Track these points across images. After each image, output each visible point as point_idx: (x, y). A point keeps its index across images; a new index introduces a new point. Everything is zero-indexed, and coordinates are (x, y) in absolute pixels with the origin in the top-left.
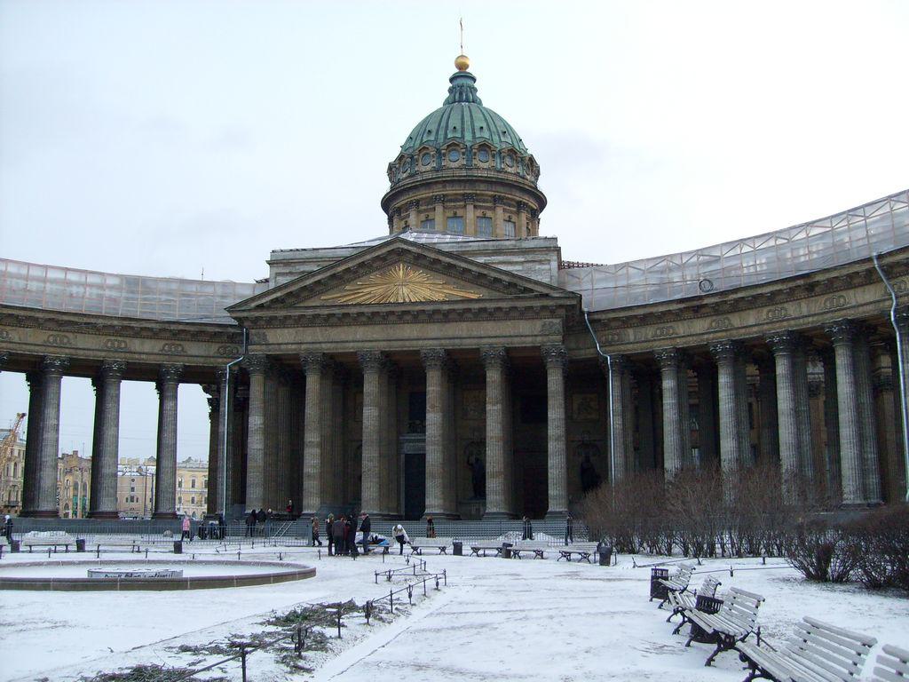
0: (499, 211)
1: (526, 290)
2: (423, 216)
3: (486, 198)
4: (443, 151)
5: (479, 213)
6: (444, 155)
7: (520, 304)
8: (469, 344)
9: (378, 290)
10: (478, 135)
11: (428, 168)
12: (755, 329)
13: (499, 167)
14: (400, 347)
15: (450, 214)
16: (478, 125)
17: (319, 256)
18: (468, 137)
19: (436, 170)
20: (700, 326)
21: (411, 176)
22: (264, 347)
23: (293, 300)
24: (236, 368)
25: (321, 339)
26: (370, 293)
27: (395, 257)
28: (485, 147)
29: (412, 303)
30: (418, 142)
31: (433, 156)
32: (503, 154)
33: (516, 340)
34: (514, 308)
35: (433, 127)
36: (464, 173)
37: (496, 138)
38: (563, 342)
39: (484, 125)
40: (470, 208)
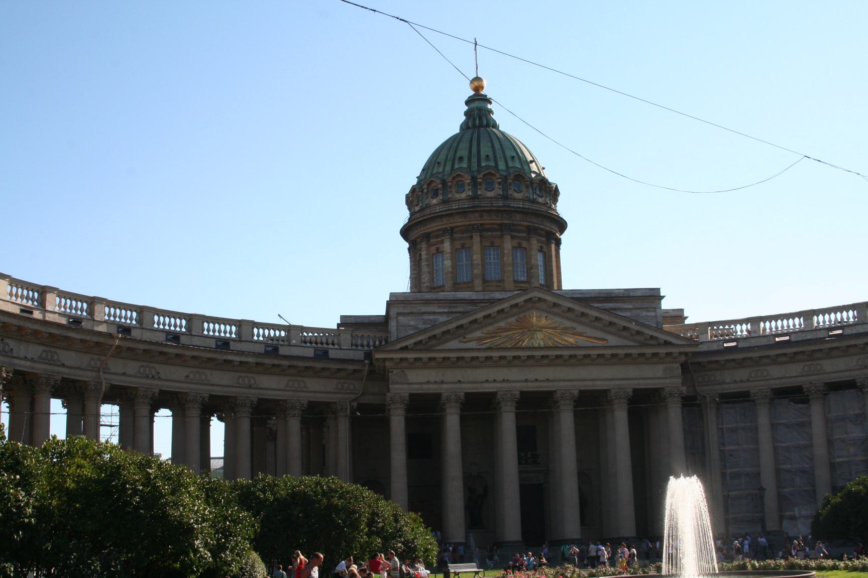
1: (652, 337)
3: (520, 228)
4: (480, 180)
5: (515, 243)
6: (480, 184)
7: (649, 351)
8: (600, 385)
10: (510, 165)
11: (463, 195)
12: (847, 373)
13: (531, 197)
14: (537, 387)
17: (440, 298)
18: (502, 166)
21: (444, 202)
22: (406, 386)
24: (355, 404)
26: (506, 336)
29: (547, 348)
30: (448, 168)
31: (468, 184)
32: (535, 185)
33: (641, 382)
35: (463, 152)
36: (501, 203)
38: (683, 384)
40: (507, 238)
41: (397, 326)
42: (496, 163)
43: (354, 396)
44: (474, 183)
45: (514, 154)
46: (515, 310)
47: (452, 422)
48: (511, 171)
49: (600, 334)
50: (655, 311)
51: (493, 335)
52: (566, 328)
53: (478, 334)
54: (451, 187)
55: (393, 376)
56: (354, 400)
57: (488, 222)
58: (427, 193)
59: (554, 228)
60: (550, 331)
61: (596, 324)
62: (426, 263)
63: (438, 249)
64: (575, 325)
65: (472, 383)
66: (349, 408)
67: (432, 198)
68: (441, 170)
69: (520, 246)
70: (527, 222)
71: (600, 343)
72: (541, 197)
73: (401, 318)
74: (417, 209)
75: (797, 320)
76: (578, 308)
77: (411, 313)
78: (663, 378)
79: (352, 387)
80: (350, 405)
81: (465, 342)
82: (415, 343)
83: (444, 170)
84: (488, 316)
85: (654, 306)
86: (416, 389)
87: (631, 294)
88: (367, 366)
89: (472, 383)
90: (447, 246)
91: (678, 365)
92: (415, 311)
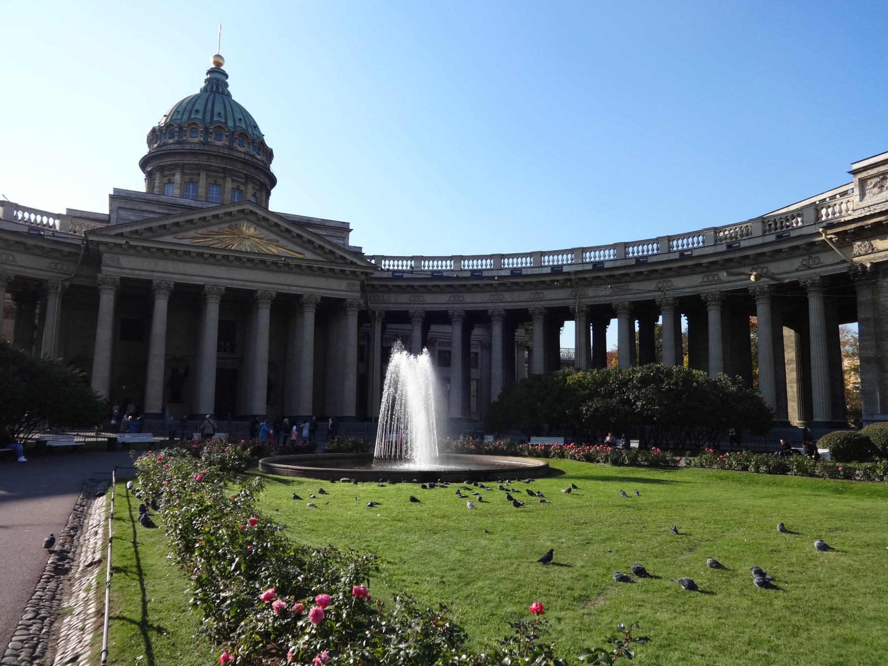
0: (250, 187)
2: (187, 178)
3: (241, 175)
5: (235, 185)
8: (294, 290)
10: (238, 124)
11: (196, 140)
12: (481, 305)
15: (211, 181)
18: (230, 123)
21: (179, 143)
22: (118, 270)
23: (150, 234)
24: (67, 284)
25: (172, 270)
26: (218, 239)
27: (242, 216)
28: (244, 135)
30: (186, 117)
31: (201, 132)
32: (255, 144)
35: (200, 106)
36: (226, 151)
37: (250, 130)
39: (242, 118)
40: (229, 180)
41: (117, 218)
43: (67, 277)
44: (206, 131)
45: (242, 118)
46: (227, 218)
47: (161, 305)
48: (238, 129)
49: (298, 249)
50: (344, 240)
51: (205, 236)
52: (270, 240)
53: (192, 233)
54: (186, 132)
55: (106, 257)
56: (66, 280)
57: (214, 164)
58: (165, 134)
59: (267, 181)
60: (257, 240)
61: (296, 240)
62: (158, 190)
63: (169, 179)
64: (278, 238)
65: (183, 274)
66: (60, 287)
67: (170, 138)
68: (179, 117)
69: (238, 189)
70: (245, 170)
71: (299, 256)
72: (259, 155)
73: (122, 212)
74: (155, 145)
75: (448, 262)
77: (132, 209)
78: (347, 291)
79: (65, 268)
80: (62, 284)
81: (179, 239)
82: (131, 232)
83: (181, 118)
85: (344, 236)
86: (127, 273)
87: (326, 224)
88: (83, 251)
89: (183, 274)
90: (177, 178)
91: (358, 282)
92: (136, 207)
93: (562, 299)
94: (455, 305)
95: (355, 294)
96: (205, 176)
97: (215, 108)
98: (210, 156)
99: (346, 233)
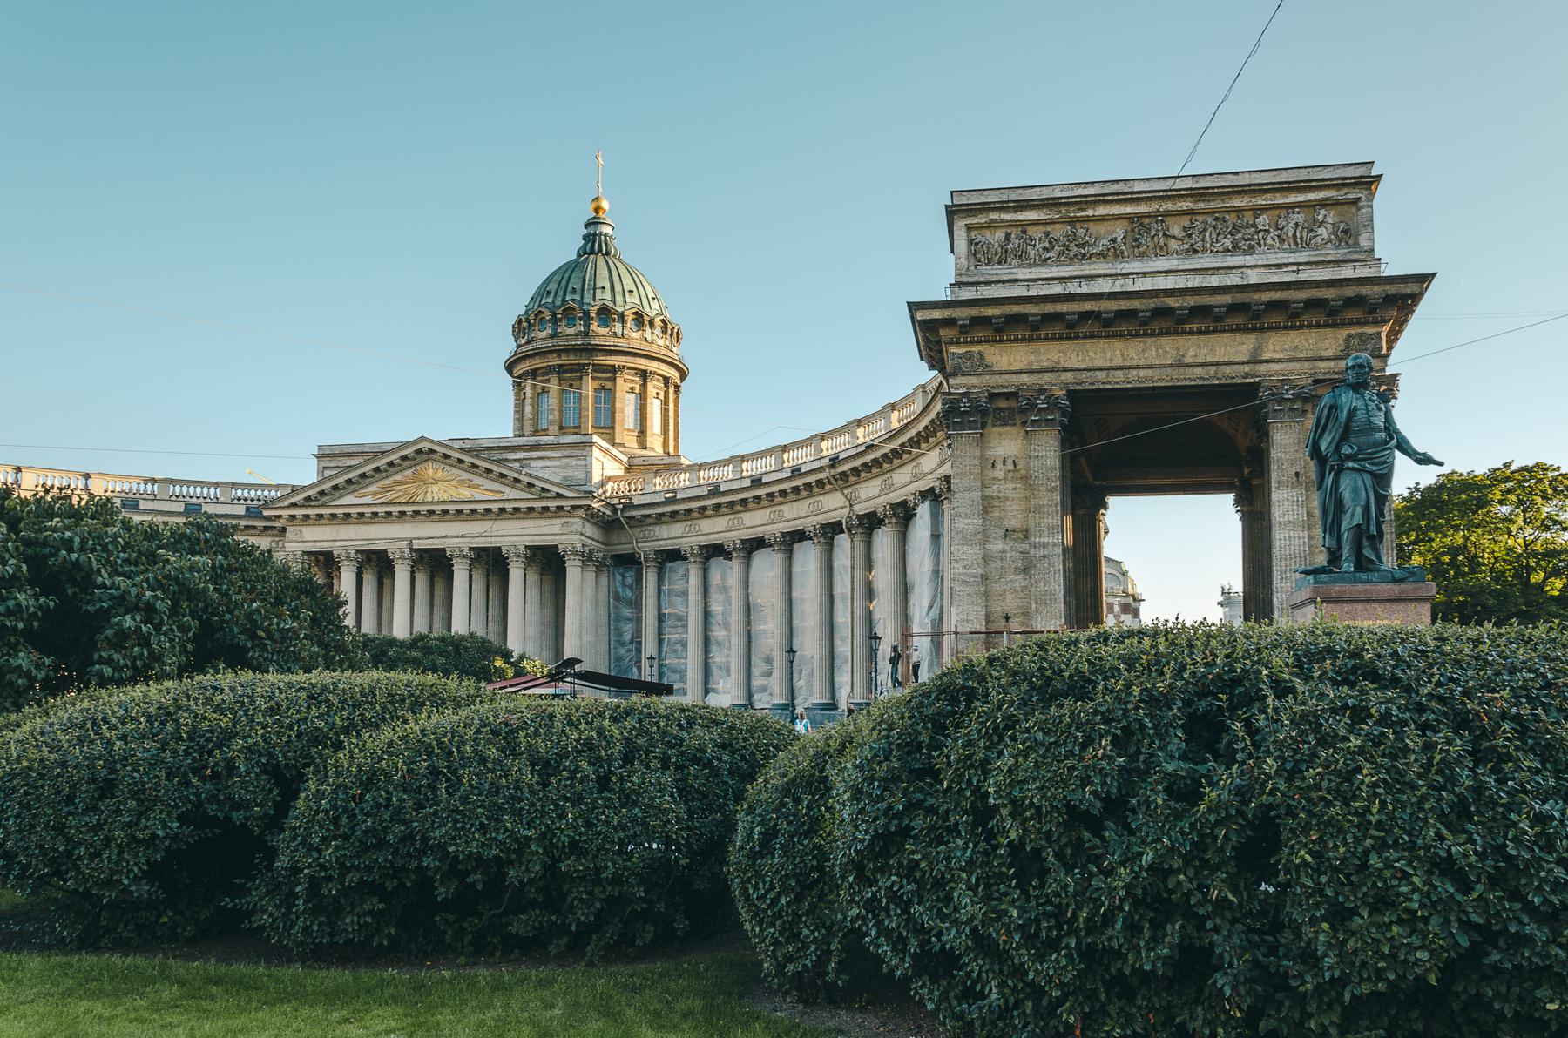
1: (544, 490)
4: (559, 316)
5: (596, 384)
6: (560, 320)
7: (538, 505)
9: (411, 488)
10: (598, 296)
11: (544, 334)
14: (430, 544)
16: (599, 284)
19: (552, 337)
20: (721, 523)
25: (354, 537)
26: (401, 490)
34: (531, 509)
35: (553, 287)
37: (619, 299)
39: (607, 285)
42: (613, 295)
44: (555, 321)
46: (407, 463)
52: (462, 481)
53: (374, 488)
54: (534, 326)
64: (471, 477)
71: (497, 496)
76: (468, 459)
84: (377, 470)
86: (309, 547)
93: (834, 510)
94: (734, 533)
95: (574, 536)
96: (557, 380)
97: (572, 280)
98: (560, 352)
99: (588, 448)
